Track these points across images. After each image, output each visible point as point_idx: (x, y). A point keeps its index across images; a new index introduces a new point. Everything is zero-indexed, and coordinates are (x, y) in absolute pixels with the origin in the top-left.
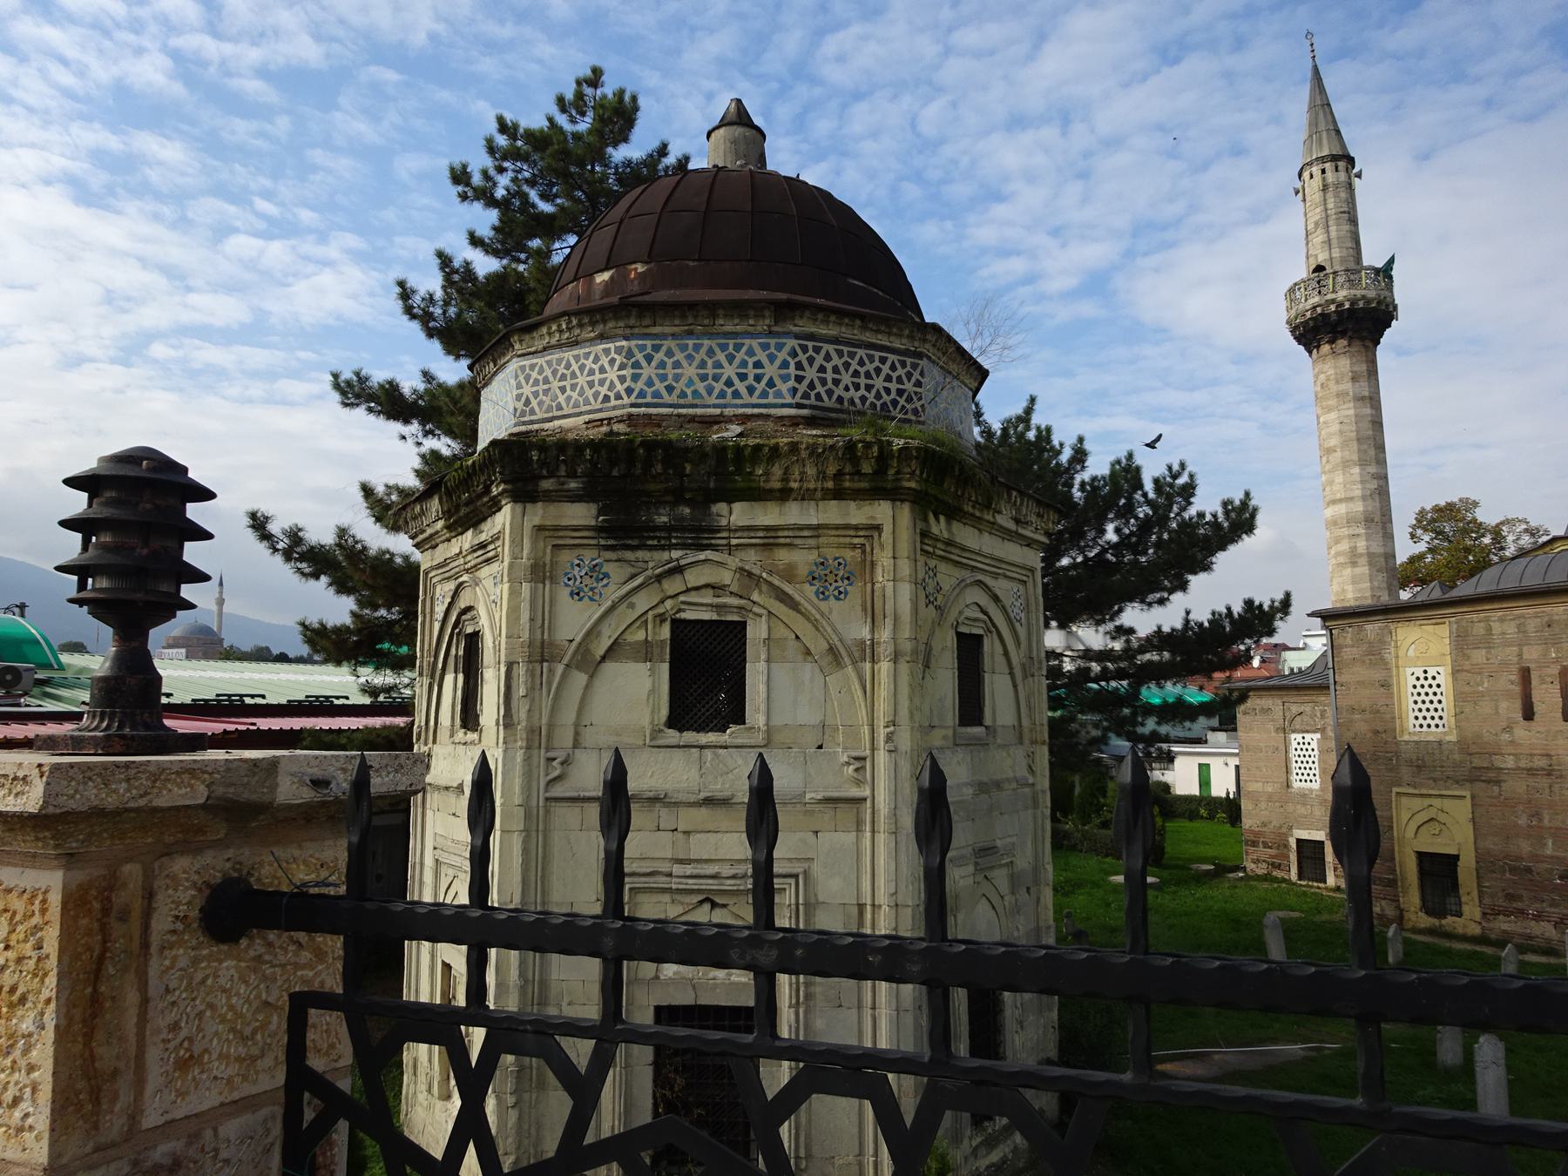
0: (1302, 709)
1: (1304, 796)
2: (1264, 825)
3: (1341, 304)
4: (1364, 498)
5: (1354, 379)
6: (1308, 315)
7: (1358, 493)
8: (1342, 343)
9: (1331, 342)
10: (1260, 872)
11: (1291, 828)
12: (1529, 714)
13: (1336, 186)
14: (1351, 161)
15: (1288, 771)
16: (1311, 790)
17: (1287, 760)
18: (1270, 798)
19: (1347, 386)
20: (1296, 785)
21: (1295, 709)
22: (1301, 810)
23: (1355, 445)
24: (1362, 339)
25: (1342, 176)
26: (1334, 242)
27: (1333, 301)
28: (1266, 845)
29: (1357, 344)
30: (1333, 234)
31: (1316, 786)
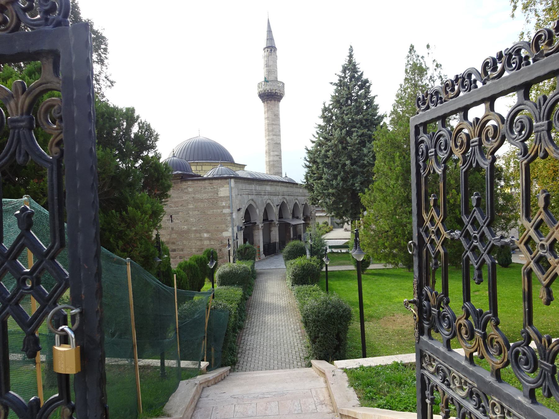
24: (267, 101)
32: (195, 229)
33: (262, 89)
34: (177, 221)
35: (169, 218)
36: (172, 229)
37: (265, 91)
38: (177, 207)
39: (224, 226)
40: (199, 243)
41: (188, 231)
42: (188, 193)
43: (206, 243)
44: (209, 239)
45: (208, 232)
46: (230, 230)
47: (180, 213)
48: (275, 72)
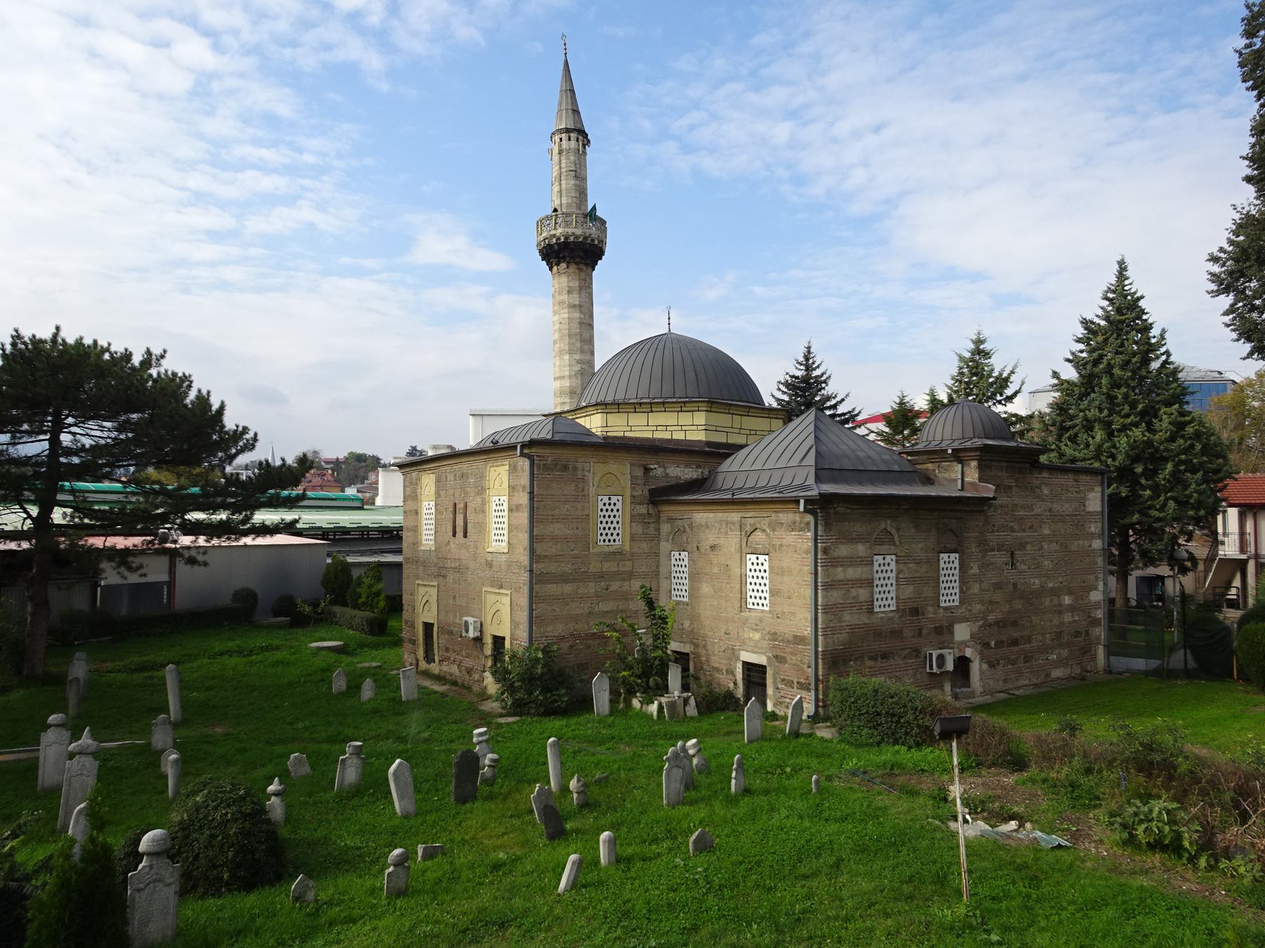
3: (559, 239)
4: (570, 377)
5: (569, 292)
7: (567, 373)
8: (563, 265)
12: (454, 535)
13: (568, 151)
14: (585, 135)
19: (565, 297)
23: (567, 339)
24: (577, 263)
25: (573, 144)
26: (564, 192)
27: (554, 236)
29: (573, 268)
30: (564, 186)
32: (1051, 585)
33: (579, 232)
34: (1023, 567)
35: (1007, 559)
36: (1015, 585)
37: (586, 238)
38: (1024, 531)
39: (1092, 577)
40: (1056, 621)
41: (1041, 592)
42: (1041, 499)
43: (1067, 618)
44: (1072, 609)
45: (1070, 593)
46: (1101, 587)
47: (1028, 547)
48: (582, 193)
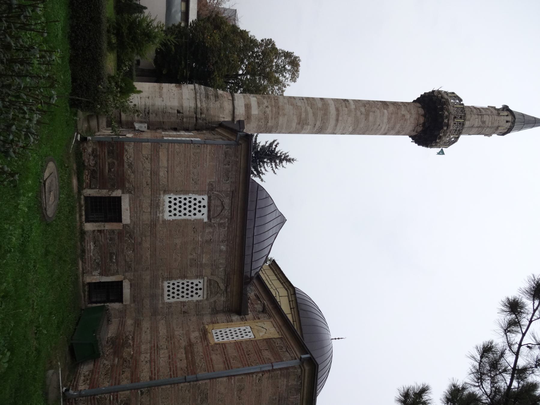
0: (227, 207)
1: (158, 206)
2: (130, 165)
6: (446, 121)
9: (424, 124)
10: (85, 157)
11: (130, 193)
15: (176, 192)
16: (163, 212)
17: (187, 192)
18: (154, 173)
20: (166, 198)
21: (227, 201)
22: (146, 203)
28: (111, 165)
31: (167, 216)
